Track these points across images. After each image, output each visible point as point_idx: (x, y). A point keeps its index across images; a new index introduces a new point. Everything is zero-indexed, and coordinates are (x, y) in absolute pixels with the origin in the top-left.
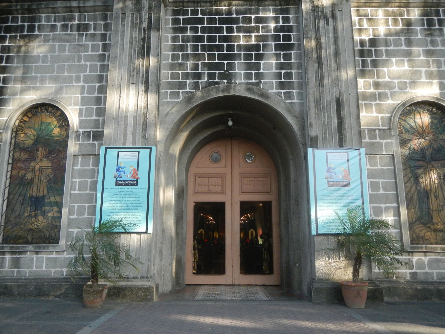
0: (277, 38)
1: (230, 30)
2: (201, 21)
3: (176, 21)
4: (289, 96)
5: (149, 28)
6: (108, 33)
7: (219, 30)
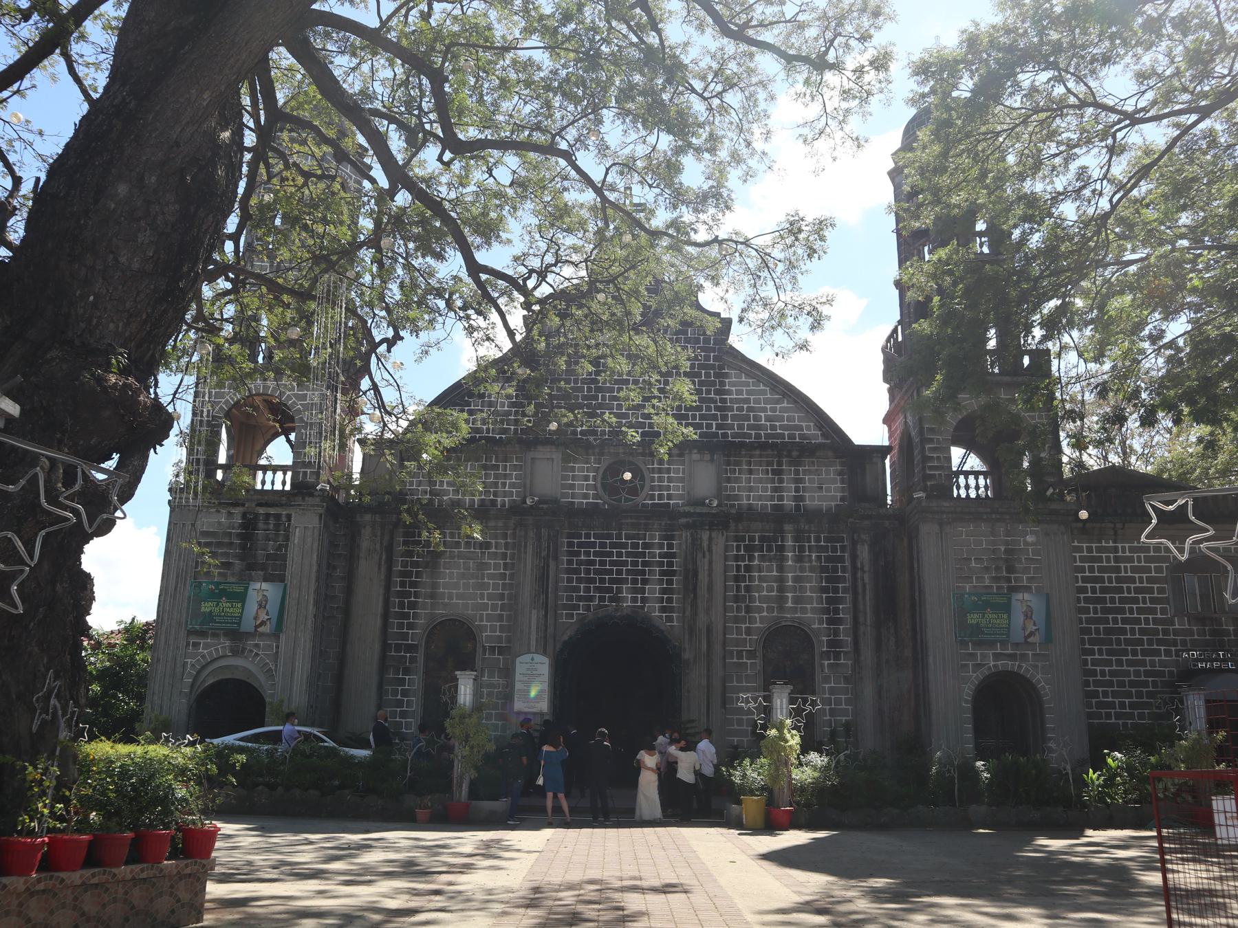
0: (661, 564)
1: (620, 555)
2: (593, 545)
3: (570, 545)
4: (670, 619)
5: (548, 555)
6: (509, 552)
7: (610, 554)
